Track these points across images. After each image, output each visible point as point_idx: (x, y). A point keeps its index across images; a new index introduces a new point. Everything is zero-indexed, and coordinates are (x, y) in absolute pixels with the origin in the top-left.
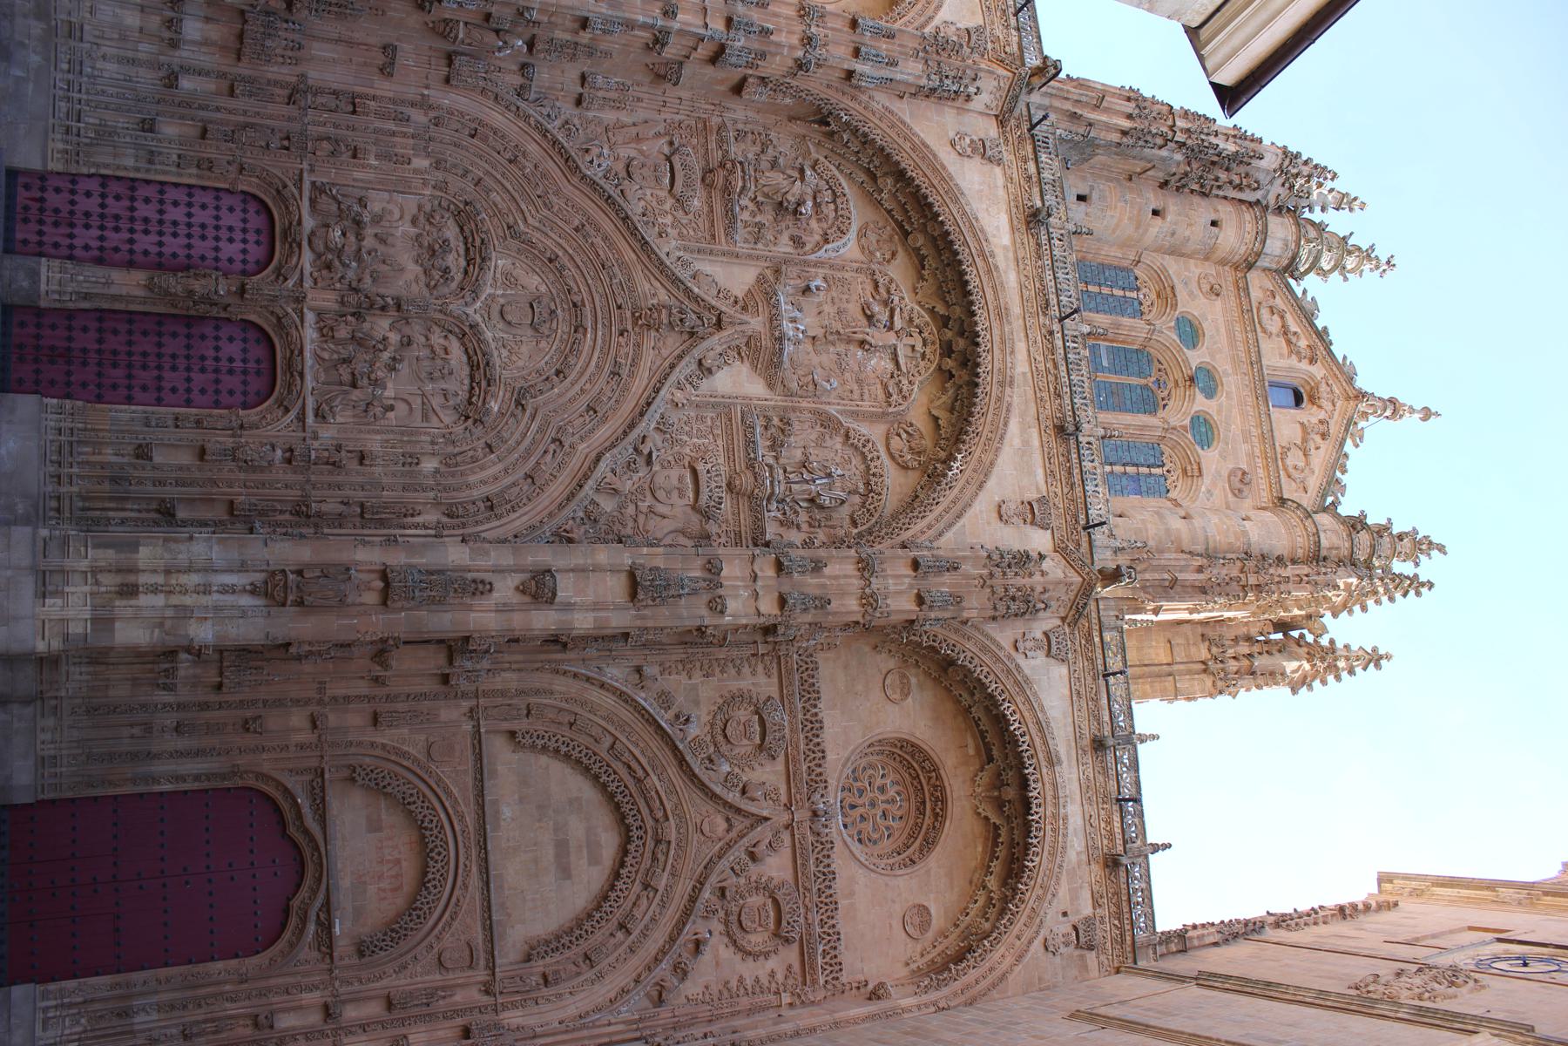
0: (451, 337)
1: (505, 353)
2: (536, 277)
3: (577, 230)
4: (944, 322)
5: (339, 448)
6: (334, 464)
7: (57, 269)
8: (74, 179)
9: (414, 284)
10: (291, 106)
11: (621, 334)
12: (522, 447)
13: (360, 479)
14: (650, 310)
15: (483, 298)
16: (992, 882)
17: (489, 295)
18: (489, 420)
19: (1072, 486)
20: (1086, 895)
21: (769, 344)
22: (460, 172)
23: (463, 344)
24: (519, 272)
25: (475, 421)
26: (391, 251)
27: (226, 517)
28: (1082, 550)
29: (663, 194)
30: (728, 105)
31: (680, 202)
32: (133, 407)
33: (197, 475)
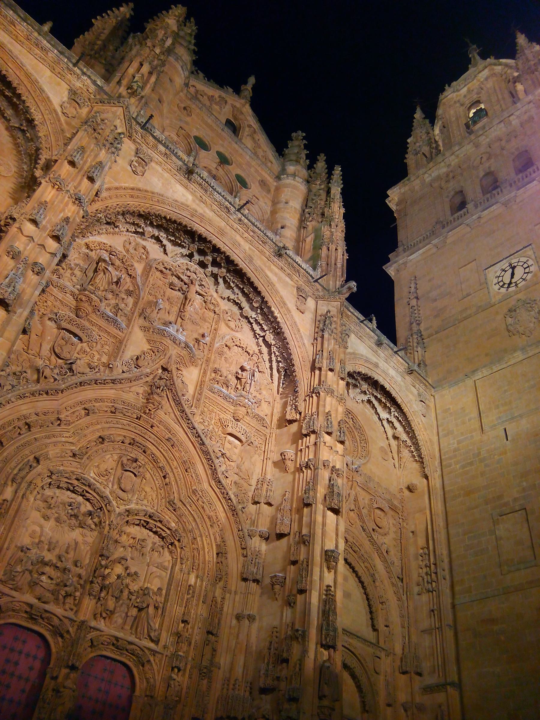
1: (145, 502)
3: (88, 414)
4: (191, 256)
5: (178, 635)
9: (86, 539)
11: (152, 427)
12: (198, 520)
14: (147, 403)
16: (384, 415)
17: (110, 493)
19: (298, 271)
20: (412, 388)
21: (184, 352)
24: (103, 467)
25: (179, 541)
26: (60, 543)
28: (320, 290)
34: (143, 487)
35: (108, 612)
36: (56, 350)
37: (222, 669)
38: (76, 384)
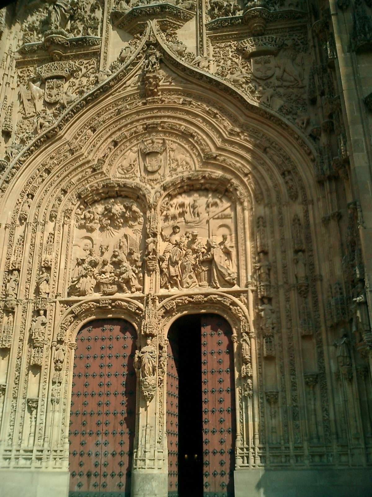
0: (172, 202)
1: (180, 169)
2: (127, 154)
6: (269, 270)
7: (142, 463)
8: (73, 454)
9: (135, 228)
10: (16, 310)
11: (163, 101)
13: (279, 254)
15: (144, 185)
18: (228, 176)
22: (57, 202)
23: (175, 196)
24: (126, 164)
27: (314, 341)
29: (67, 84)
30: (7, 48)
31: (72, 74)
32: (238, 407)
33: (286, 360)
34: (173, 158)
35: (175, 278)
36: (47, 100)
37: (325, 280)
38: (69, 114)
